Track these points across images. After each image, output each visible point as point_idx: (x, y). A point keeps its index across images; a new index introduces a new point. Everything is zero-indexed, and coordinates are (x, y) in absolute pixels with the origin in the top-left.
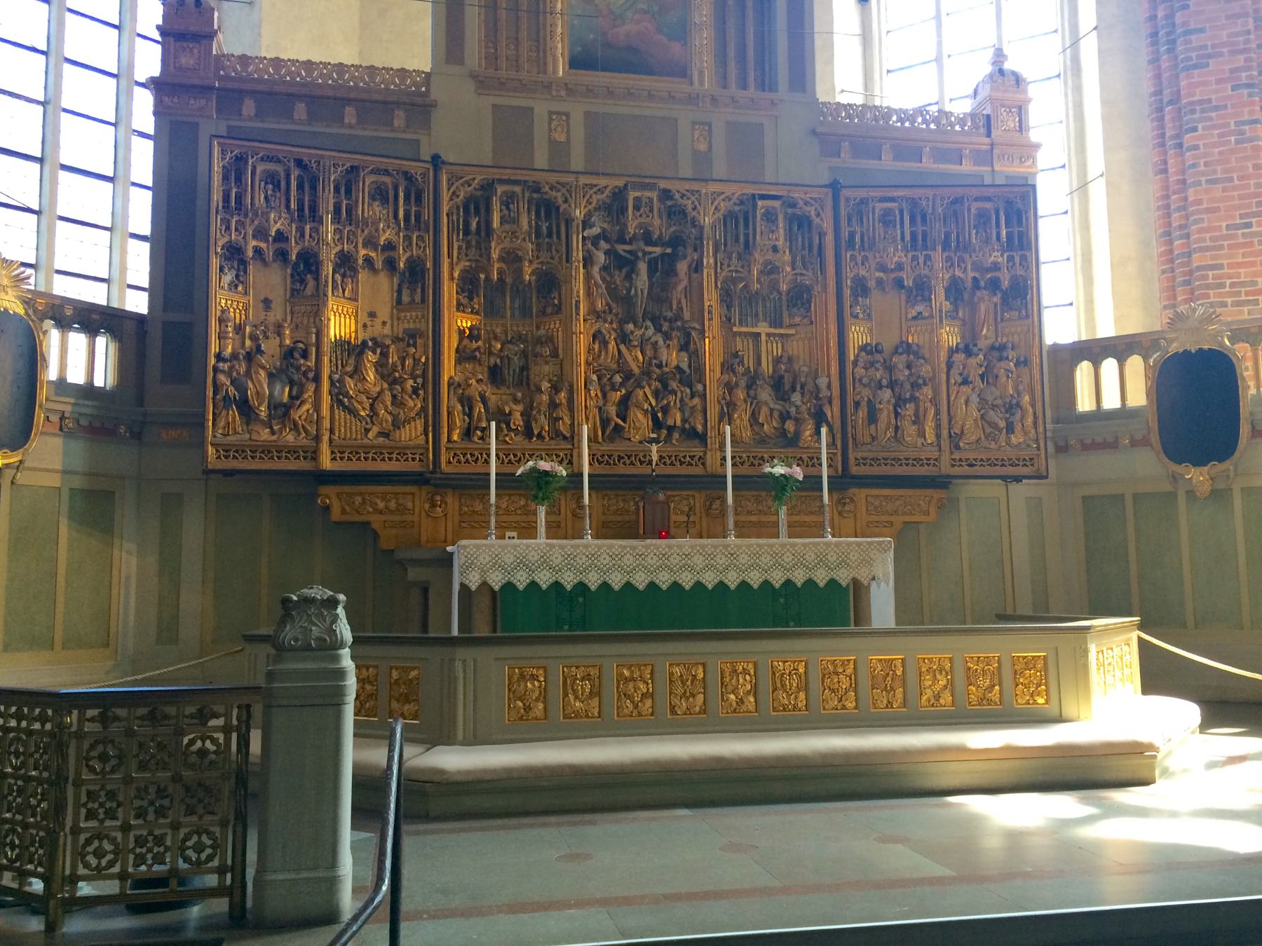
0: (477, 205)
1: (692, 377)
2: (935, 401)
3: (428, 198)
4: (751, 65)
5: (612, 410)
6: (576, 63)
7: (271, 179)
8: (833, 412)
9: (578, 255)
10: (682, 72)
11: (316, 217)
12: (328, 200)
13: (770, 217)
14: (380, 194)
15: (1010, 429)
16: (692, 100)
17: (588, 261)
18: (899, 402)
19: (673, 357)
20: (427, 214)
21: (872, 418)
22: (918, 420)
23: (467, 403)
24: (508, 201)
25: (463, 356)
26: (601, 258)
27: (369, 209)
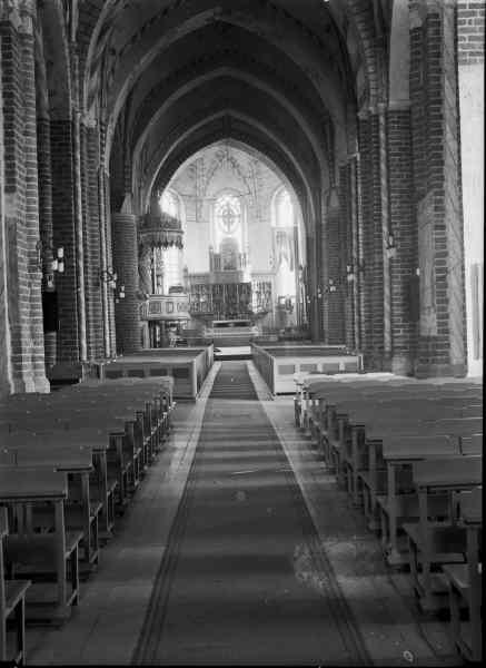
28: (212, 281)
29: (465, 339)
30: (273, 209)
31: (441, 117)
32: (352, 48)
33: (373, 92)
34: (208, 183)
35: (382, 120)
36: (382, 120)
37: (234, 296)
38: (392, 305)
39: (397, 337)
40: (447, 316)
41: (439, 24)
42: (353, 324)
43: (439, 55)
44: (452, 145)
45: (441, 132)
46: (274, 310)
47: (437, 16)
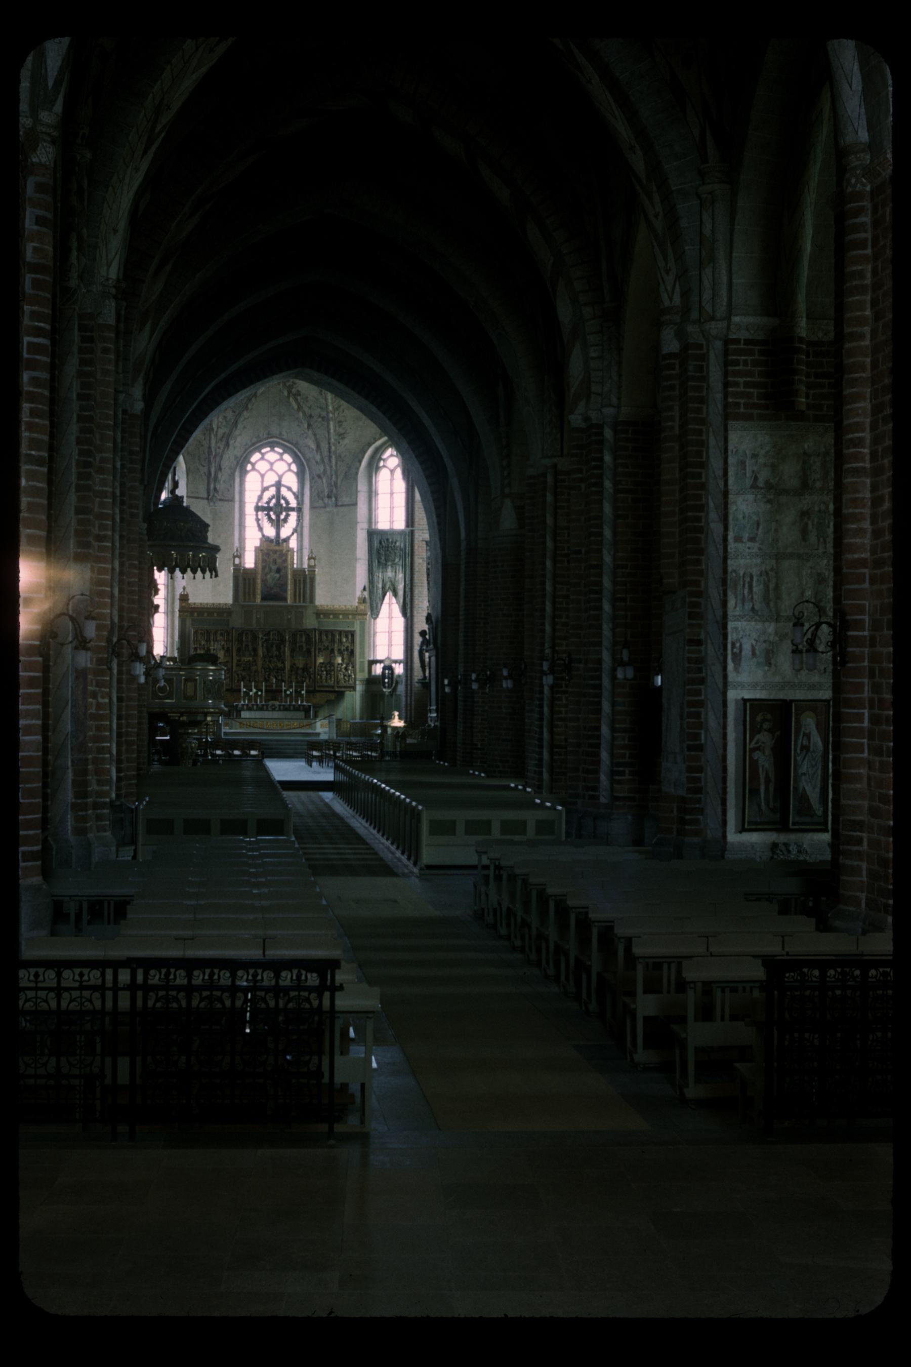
0: (241, 635)
1: (283, 669)
2: (334, 675)
3: (230, 635)
4: (302, 597)
5: (266, 676)
6: (264, 598)
7: (201, 634)
8: (312, 676)
9: (260, 645)
10: (285, 599)
11: (210, 641)
12: (212, 638)
13: (301, 636)
14: (221, 634)
15: (349, 681)
16: (287, 607)
17: (262, 646)
18: (327, 674)
19: (280, 665)
20: (230, 638)
21: (321, 677)
22: (331, 678)
23: (238, 675)
24: (247, 634)
25: (238, 665)
26: (265, 645)
27: (219, 638)
28: (237, 622)
29: (724, 802)
30: (362, 486)
31: (703, 486)
32: (565, 312)
33: (595, 388)
34: (236, 424)
35: (608, 434)
36: (608, 434)
37: (281, 658)
38: (613, 730)
39: (619, 782)
40: (700, 770)
41: (704, 358)
42: (541, 747)
43: (702, 400)
44: (716, 527)
45: (702, 508)
46: (359, 688)
47: (700, 347)
